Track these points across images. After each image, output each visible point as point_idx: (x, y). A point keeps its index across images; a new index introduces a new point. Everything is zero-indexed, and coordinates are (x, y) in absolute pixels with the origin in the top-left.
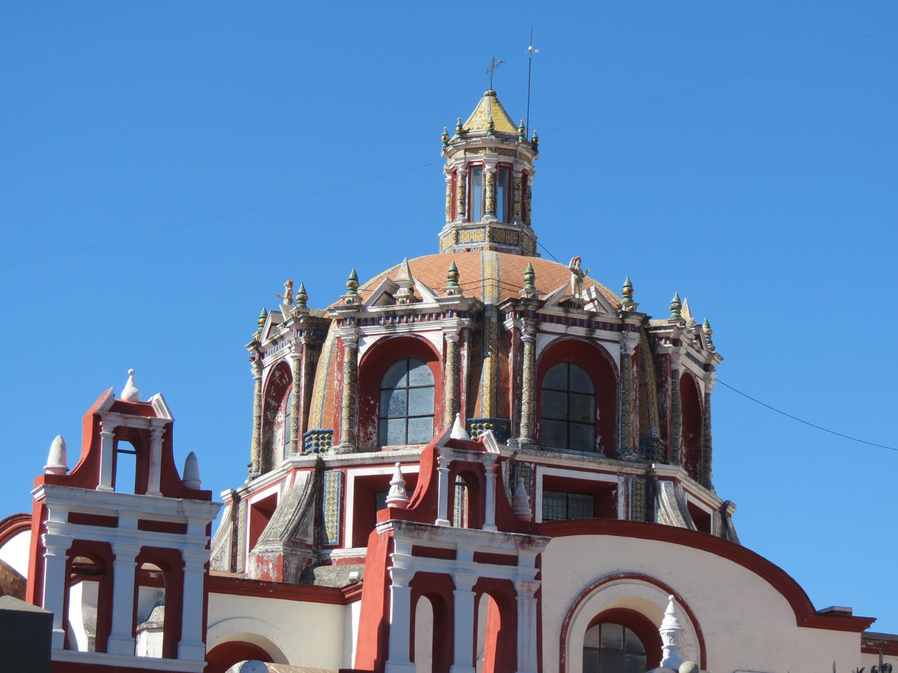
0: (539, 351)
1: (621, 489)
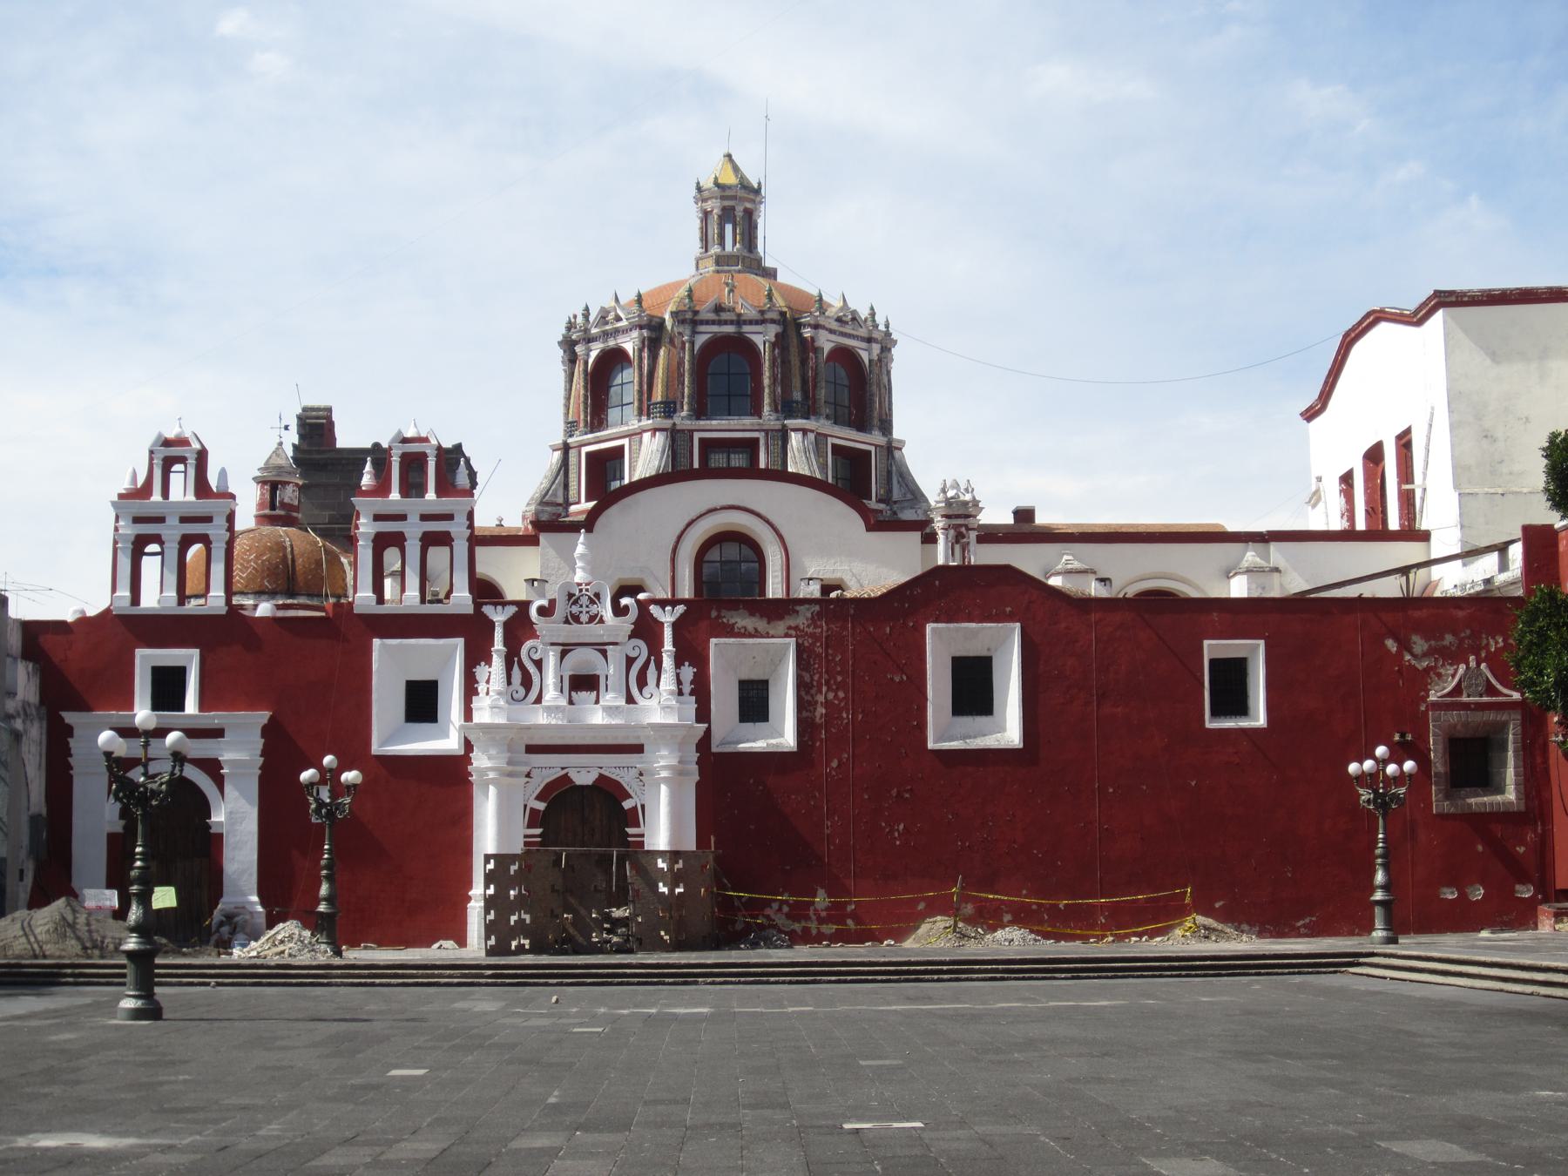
0: (697, 347)
1: (762, 442)
